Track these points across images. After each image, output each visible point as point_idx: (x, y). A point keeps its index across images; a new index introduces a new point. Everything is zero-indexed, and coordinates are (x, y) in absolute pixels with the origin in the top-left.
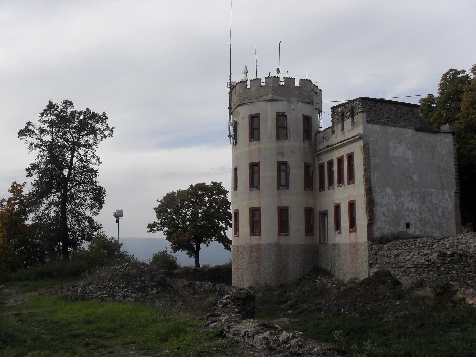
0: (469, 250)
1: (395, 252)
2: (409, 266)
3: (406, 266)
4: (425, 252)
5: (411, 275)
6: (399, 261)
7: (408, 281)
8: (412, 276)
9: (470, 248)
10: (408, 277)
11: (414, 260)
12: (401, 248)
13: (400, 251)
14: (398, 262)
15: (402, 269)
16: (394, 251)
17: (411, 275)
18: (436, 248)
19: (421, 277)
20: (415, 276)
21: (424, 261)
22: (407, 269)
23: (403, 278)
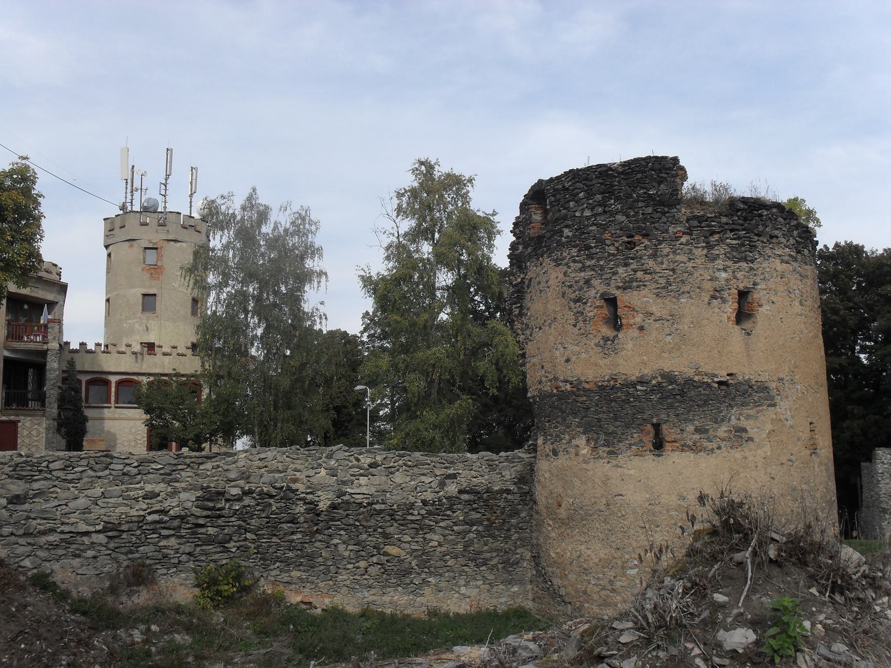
0: (294, 486)
1: (12, 487)
2: (83, 527)
3: (66, 528)
4: (149, 488)
5: (90, 553)
6: (33, 516)
7: (80, 572)
8: (95, 557)
9: (295, 481)
10: (78, 560)
11: (103, 511)
12: (49, 476)
13: (36, 486)
14: (28, 518)
15: (51, 538)
16: (12, 483)
17: (90, 553)
18: (188, 479)
19: (130, 556)
20: (109, 554)
21: (142, 513)
22: (71, 537)
23: (56, 566)
